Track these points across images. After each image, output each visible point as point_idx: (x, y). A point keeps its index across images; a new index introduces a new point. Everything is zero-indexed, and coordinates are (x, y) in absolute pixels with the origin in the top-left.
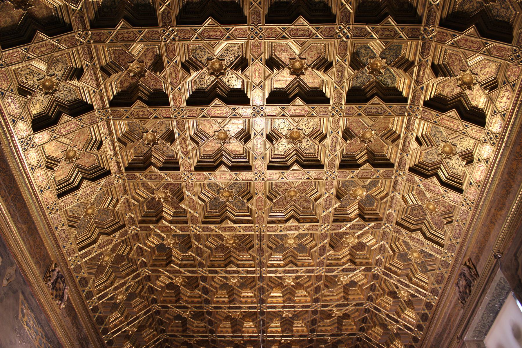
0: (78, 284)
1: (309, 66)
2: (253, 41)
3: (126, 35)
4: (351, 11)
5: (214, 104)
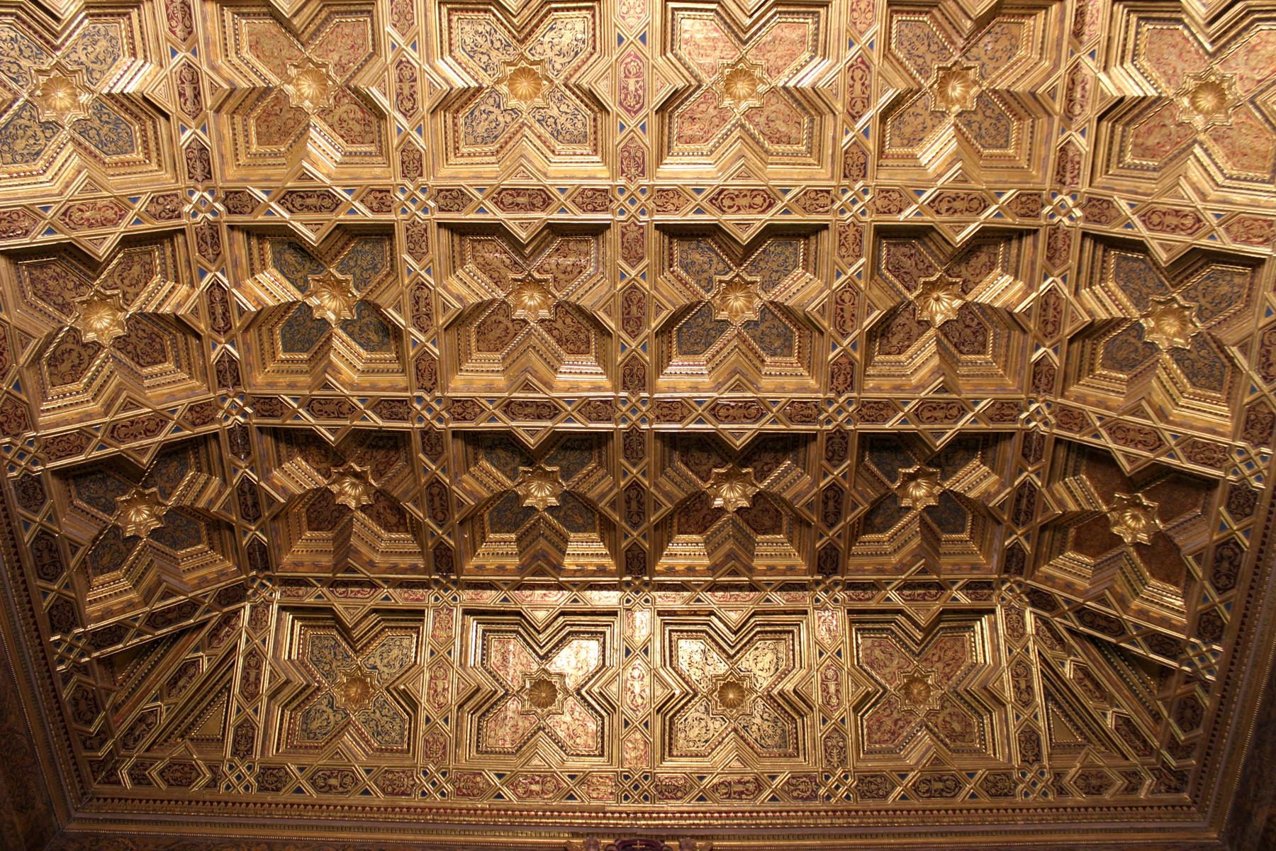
1: (504, 302)
2: (642, 394)
3: (939, 414)
4: (421, 455)
5: (751, 231)
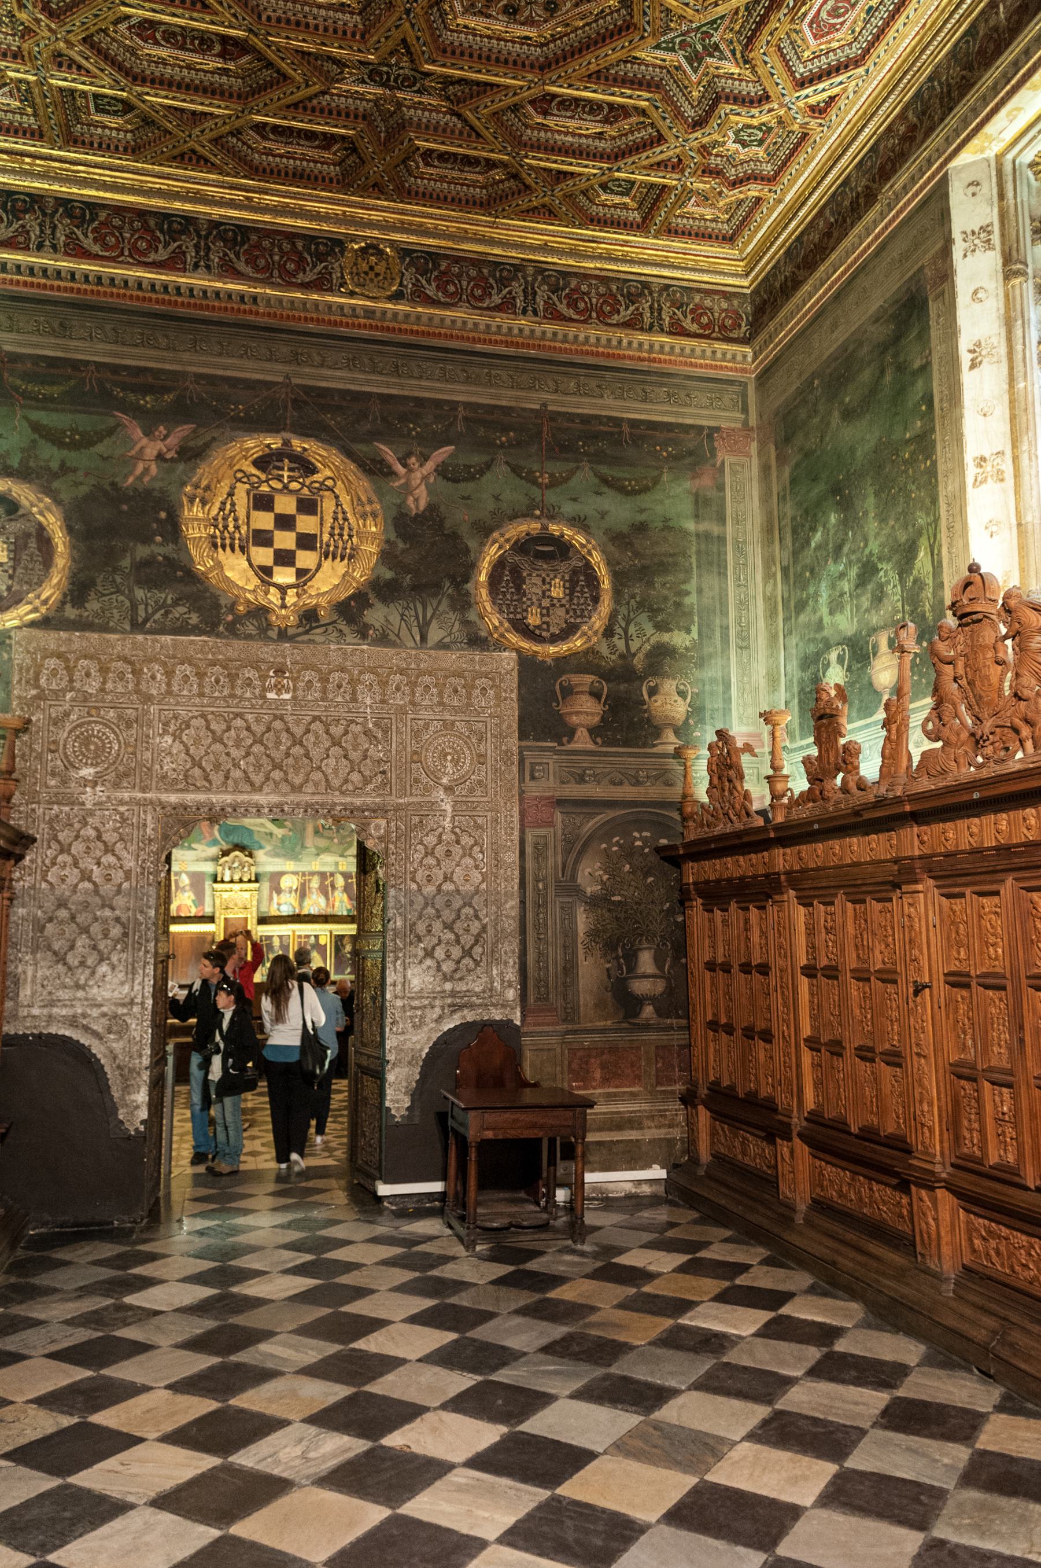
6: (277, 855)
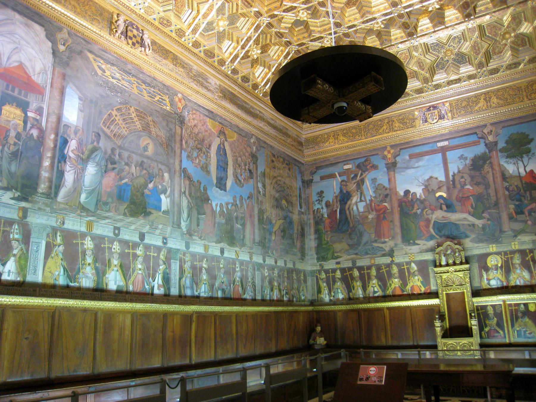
0: (160, 26)
6: (480, 241)
